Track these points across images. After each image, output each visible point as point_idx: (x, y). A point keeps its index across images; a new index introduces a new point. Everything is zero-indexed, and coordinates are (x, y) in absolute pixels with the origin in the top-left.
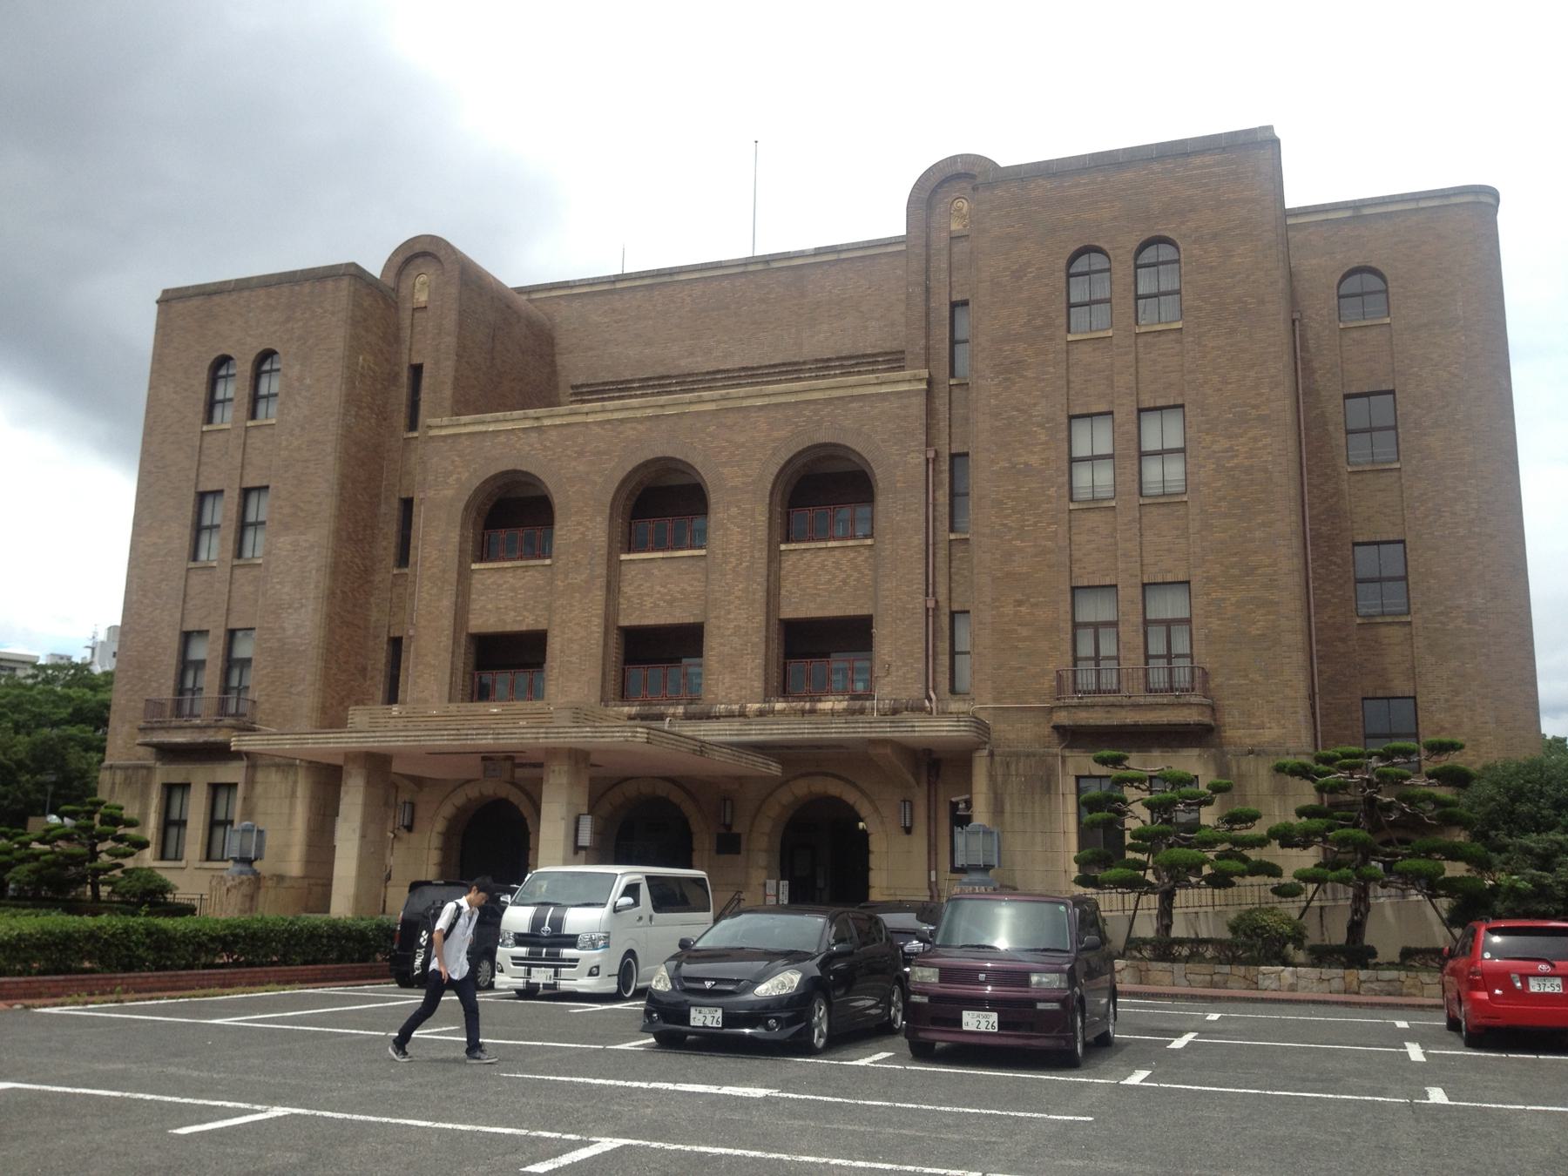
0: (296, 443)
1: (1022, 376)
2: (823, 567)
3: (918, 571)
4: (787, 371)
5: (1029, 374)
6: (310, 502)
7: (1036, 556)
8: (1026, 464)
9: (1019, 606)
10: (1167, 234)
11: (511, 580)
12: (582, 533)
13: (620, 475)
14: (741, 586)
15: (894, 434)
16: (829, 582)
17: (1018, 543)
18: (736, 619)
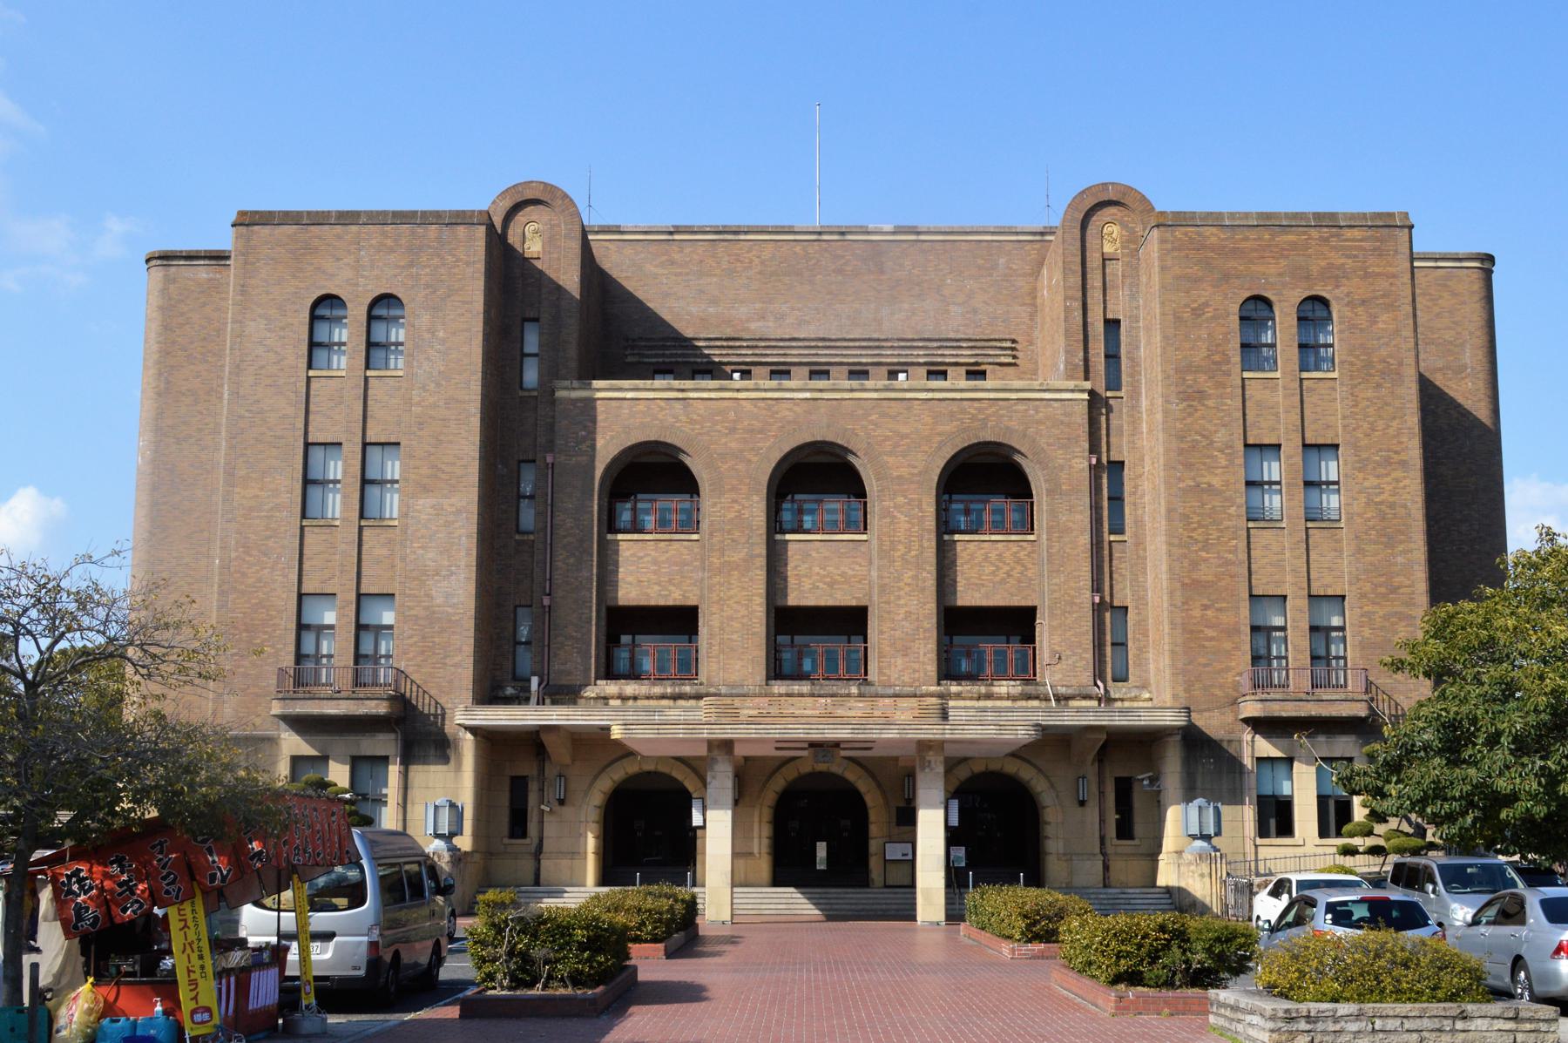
0: (431, 400)
1: (1204, 405)
2: (986, 559)
3: (1085, 569)
4: (899, 355)
5: (1210, 403)
6: (454, 464)
7: (1220, 566)
8: (1210, 485)
9: (1205, 610)
11: (653, 553)
12: (739, 512)
13: (777, 456)
14: (911, 573)
15: (1059, 439)
18: (906, 605)
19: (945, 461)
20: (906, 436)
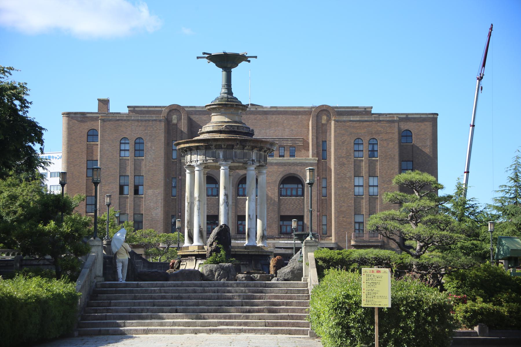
0: (151, 165)
5: (346, 166)
8: (345, 187)
10: (376, 138)
14: (272, 207)
16: (292, 207)
17: (343, 204)
19: (281, 178)
20: (271, 172)
